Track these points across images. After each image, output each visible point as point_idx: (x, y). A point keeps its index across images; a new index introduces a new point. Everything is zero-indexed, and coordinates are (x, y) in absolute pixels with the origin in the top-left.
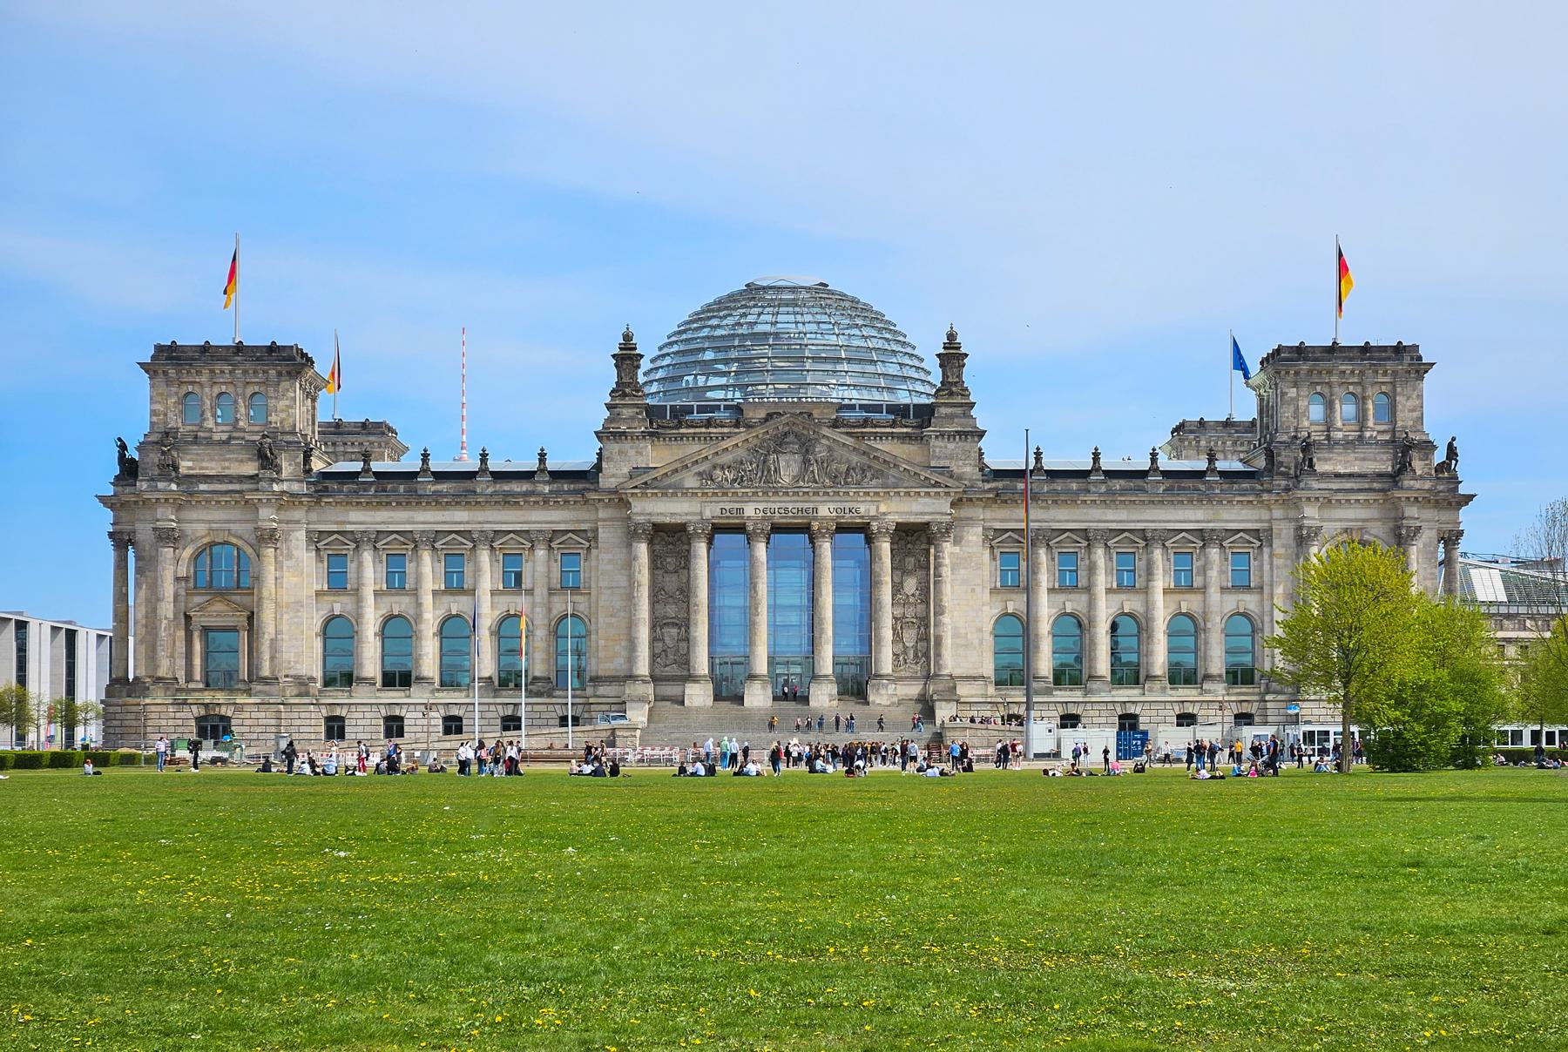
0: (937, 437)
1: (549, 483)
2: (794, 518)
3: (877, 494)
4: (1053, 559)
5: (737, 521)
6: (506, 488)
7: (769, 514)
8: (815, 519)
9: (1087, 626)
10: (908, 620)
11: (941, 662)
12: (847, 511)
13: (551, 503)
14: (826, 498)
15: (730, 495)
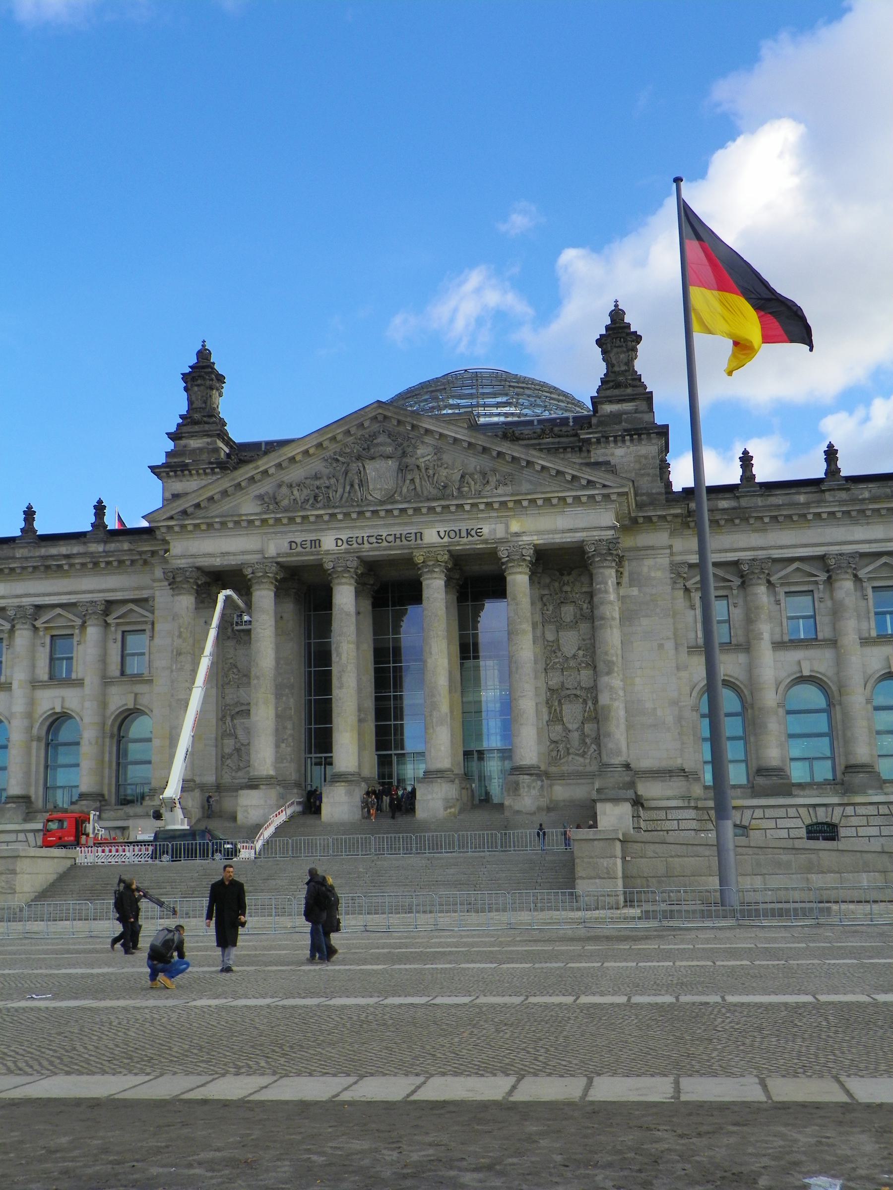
0: (598, 441)
1: (105, 542)
2: (390, 548)
3: (503, 504)
4: (778, 602)
5: (312, 558)
6: (53, 551)
7: (355, 545)
8: (419, 547)
9: (836, 694)
10: (569, 692)
11: (610, 745)
12: (464, 534)
13: (103, 565)
14: (431, 517)
15: (298, 520)
